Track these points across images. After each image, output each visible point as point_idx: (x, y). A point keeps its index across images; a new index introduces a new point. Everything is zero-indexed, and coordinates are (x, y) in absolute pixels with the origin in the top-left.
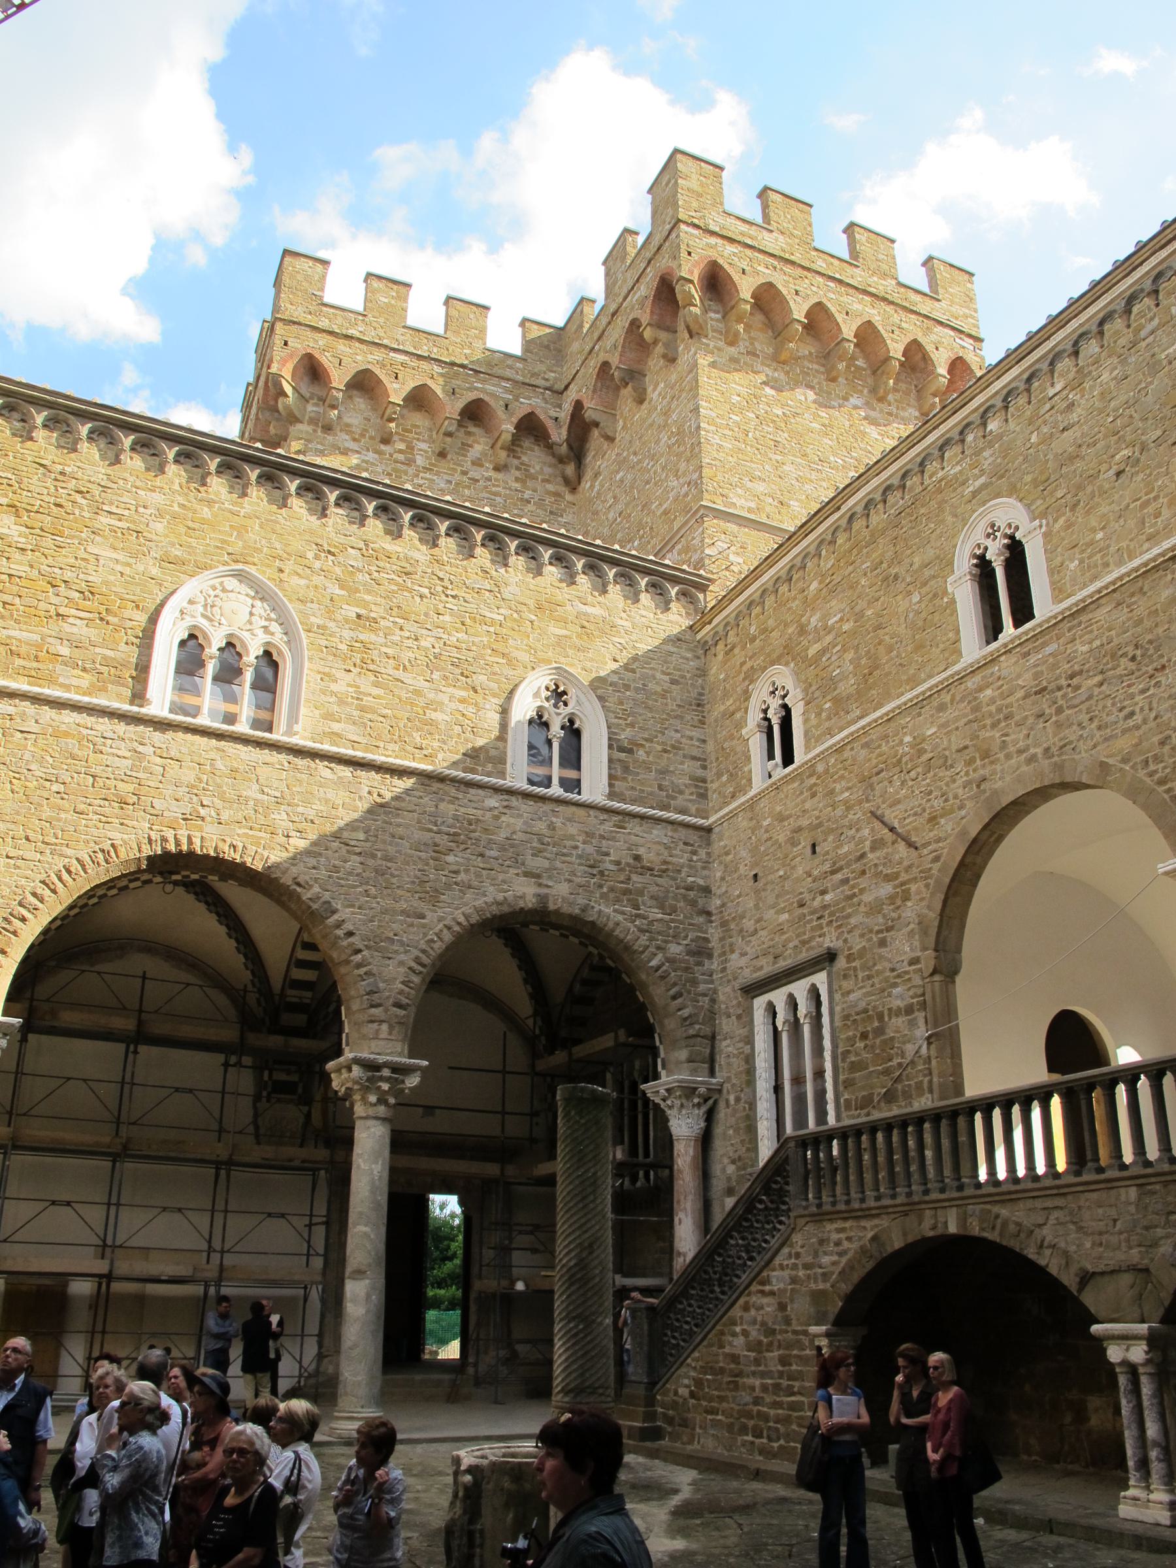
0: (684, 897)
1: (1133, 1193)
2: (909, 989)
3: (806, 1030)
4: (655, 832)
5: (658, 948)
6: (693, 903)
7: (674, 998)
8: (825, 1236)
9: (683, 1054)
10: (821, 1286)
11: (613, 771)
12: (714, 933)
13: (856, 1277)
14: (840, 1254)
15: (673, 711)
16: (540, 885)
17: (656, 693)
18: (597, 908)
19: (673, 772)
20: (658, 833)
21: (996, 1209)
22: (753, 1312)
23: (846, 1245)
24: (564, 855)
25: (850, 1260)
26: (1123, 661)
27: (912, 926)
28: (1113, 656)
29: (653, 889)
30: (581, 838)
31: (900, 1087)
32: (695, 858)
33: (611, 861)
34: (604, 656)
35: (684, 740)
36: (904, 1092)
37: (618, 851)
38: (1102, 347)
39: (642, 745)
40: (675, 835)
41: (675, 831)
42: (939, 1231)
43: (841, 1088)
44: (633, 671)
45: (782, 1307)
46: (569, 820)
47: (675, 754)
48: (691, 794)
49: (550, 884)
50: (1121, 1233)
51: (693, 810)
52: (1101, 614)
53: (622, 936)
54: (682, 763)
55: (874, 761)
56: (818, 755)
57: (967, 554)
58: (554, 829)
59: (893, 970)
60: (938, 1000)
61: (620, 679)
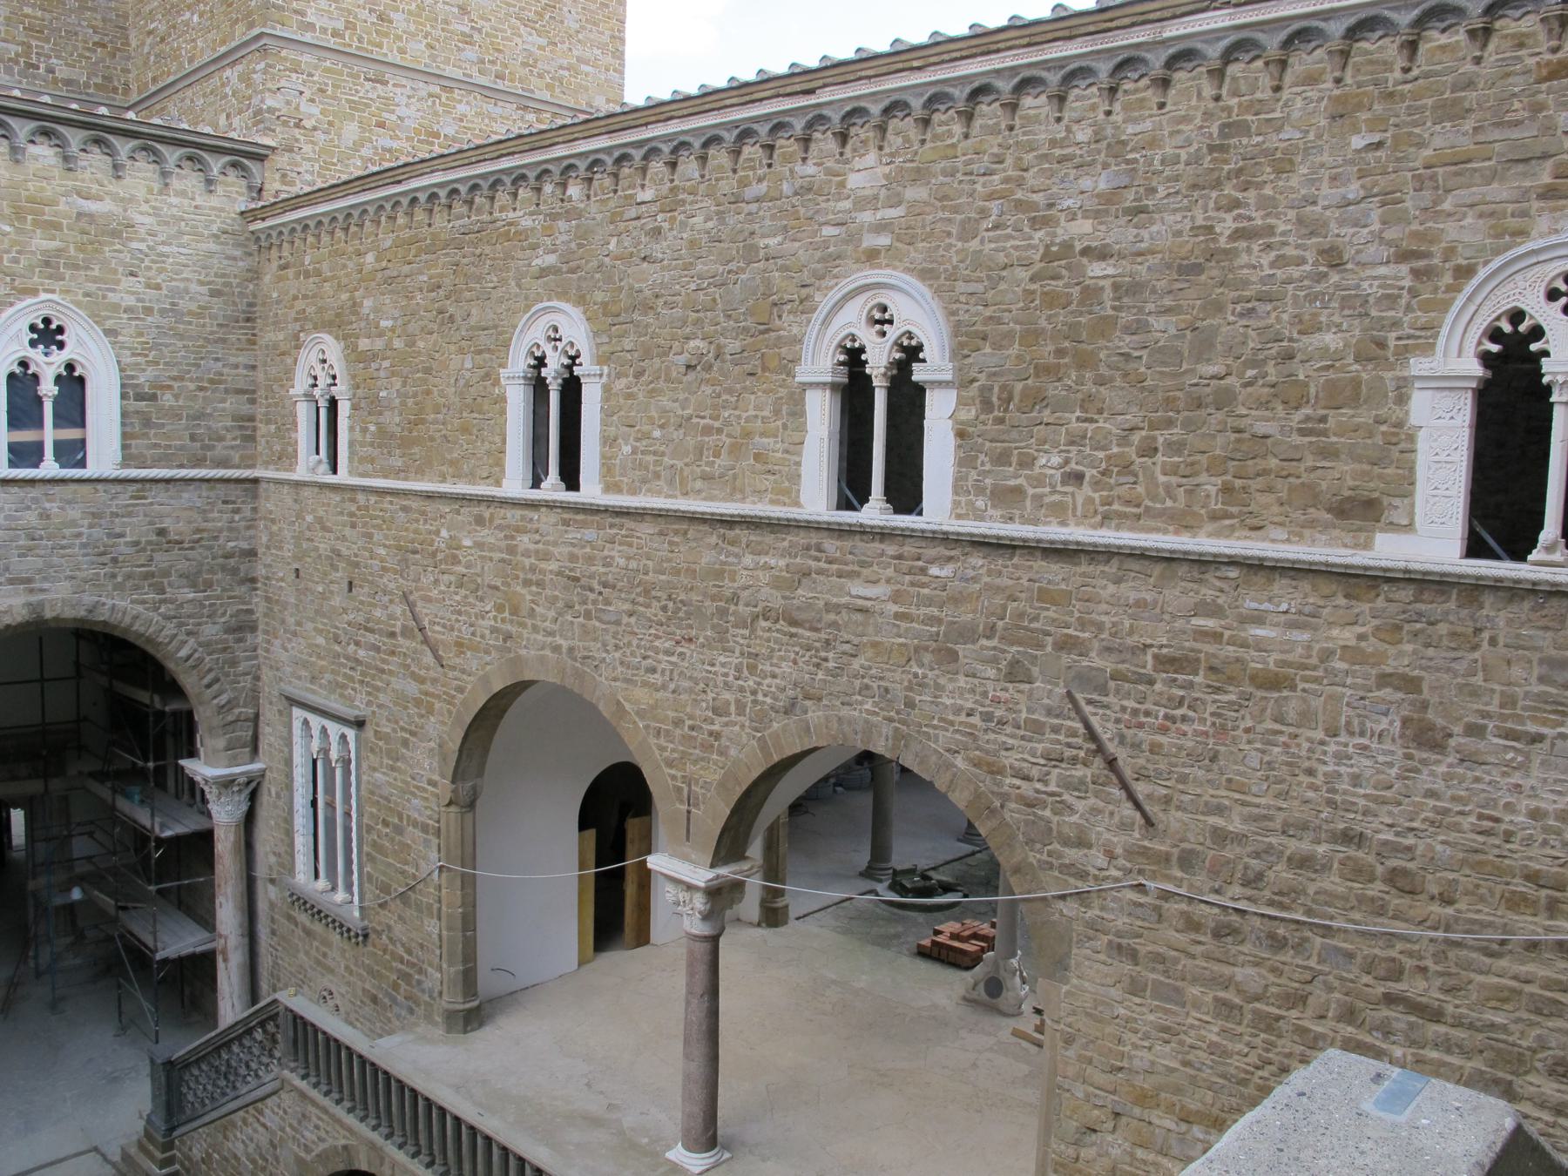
0: (223, 568)
3: (338, 773)
4: (185, 495)
5: (189, 633)
6: (234, 571)
7: (208, 686)
9: (221, 743)
11: (128, 429)
12: (258, 604)
15: (212, 333)
16: (31, 591)
17: (190, 313)
18: (110, 602)
19: (210, 415)
20: (189, 496)
24: (63, 547)
27: (432, 744)
28: (647, 592)
29: (183, 566)
30: (86, 522)
32: (237, 517)
33: (126, 543)
34: (115, 272)
35: (226, 370)
37: (136, 528)
38: (702, 176)
39: (170, 387)
40: (212, 494)
41: (212, 489)
44: (158, 287)
46: (69, 502)
47: (214, 391)
48: (234, 439)
49: (46, 585)
51: (237, 460)
53: (142, 630)
54: (223, 401)
57: (524, 351)
58: (48, 517)
60: (452, 829)
61: (139, 300)
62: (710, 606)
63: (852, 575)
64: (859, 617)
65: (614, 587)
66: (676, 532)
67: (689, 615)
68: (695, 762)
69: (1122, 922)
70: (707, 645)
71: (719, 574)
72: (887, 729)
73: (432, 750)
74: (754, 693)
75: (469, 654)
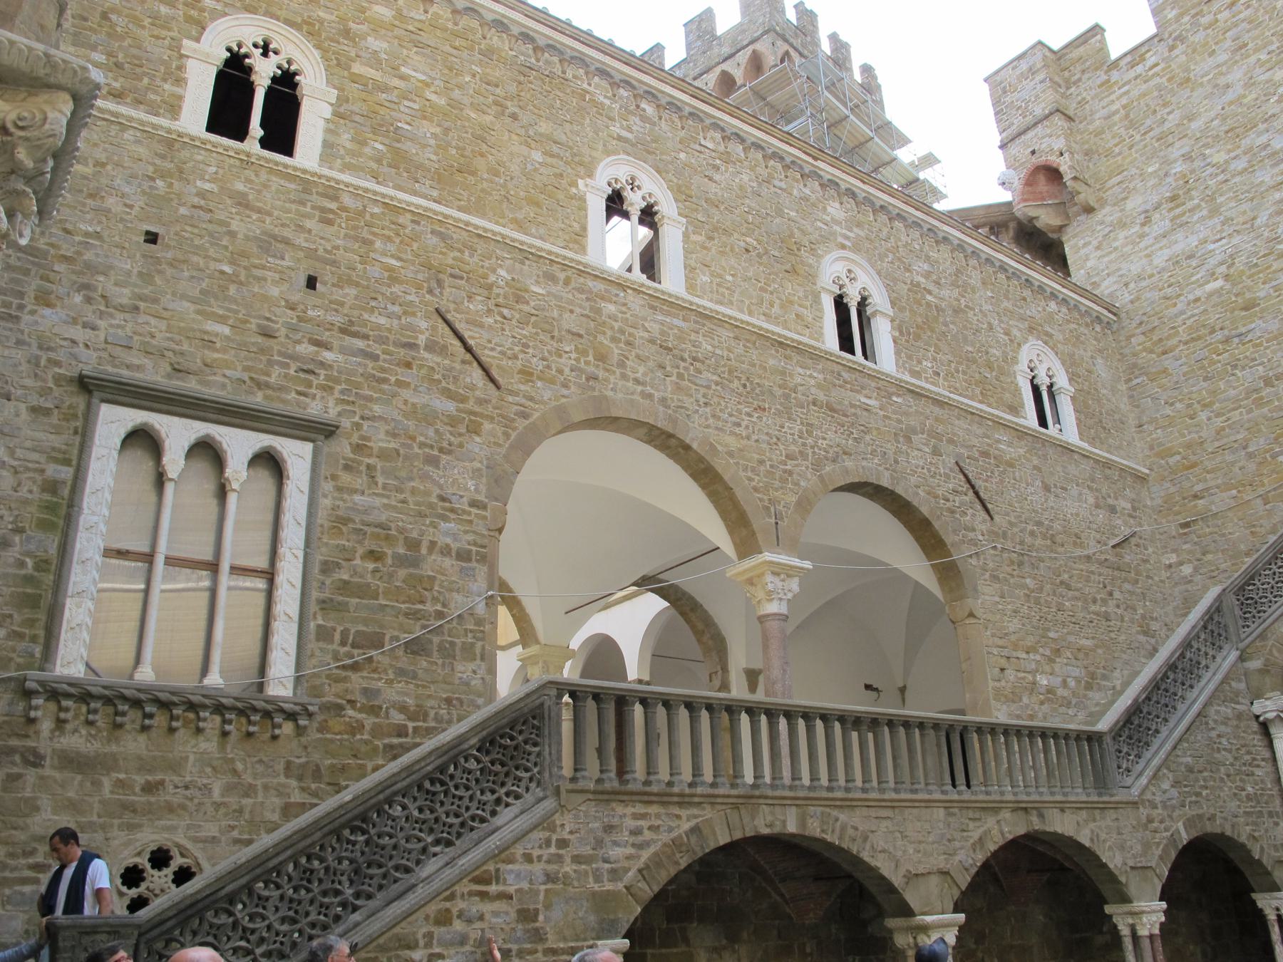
1: (941, 813)
2: (466, 532)
8: (615, 821)
10: (609, 886)
13: (663, 876)
14: (640, 846)
21: (835, 813)
22: (458, 925)
23: (648, 835)
25: (656, 854)
26: (736, 381)
31: (436, 640)
36: (441, 648)
42: (777, 830)
43: (313, 607)
45: (527, 916)
50: (933, 843)
52: (725, 334)
55: (450, 261)
56: (357, 188)
59: (443, 499)
62: (778, 392)
63: (857, 392)
64: (865, 413)
65: (703, 363)
66: (748, 341)
67: (763, 393)
68: (777, 490)
69: (991, 565)
70: (779, 413)
71: (783, 373)
72: (887, 474)
73: (479, 470)
74: (812, 447)
75: (539, 384)
